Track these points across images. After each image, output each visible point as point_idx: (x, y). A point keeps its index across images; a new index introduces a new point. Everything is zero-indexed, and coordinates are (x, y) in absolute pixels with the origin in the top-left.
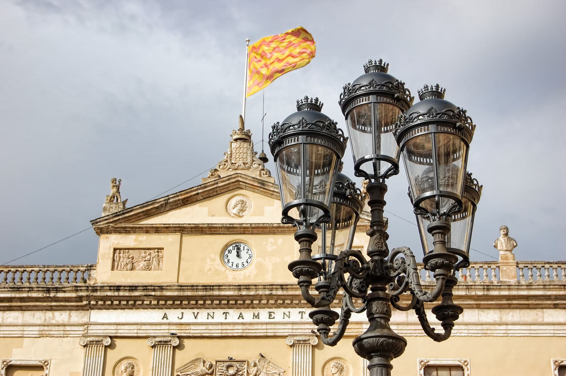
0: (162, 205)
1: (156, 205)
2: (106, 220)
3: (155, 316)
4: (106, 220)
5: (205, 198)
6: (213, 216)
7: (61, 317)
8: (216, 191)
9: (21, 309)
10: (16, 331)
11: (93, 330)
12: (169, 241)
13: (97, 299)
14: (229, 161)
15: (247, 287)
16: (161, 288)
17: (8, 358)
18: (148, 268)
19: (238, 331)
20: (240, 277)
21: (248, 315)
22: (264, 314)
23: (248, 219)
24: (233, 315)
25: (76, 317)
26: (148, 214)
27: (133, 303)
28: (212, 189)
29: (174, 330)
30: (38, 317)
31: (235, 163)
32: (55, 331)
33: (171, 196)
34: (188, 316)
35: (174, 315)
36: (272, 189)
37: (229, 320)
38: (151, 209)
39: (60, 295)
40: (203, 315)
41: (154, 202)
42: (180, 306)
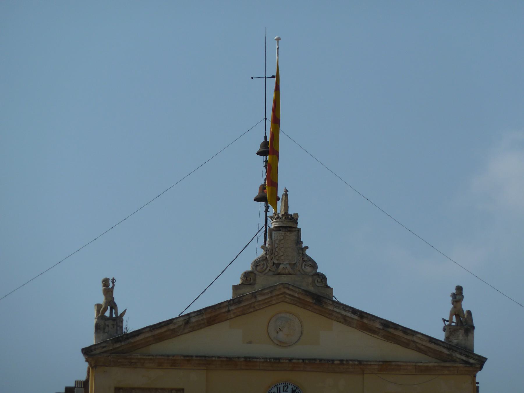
0: (180, 326)
1: (172, 327)
2: (104, 347)
4: (104, 347)
5: (238, 316)
6: (250, 342)
8: (254, 307)
14: (269, 259)
26: (160, 338)
28: (248, 304)
31: (280, 264)
33: (193, 315)
36: (331, 308)
38: (165, 332)
41: (171, 321)
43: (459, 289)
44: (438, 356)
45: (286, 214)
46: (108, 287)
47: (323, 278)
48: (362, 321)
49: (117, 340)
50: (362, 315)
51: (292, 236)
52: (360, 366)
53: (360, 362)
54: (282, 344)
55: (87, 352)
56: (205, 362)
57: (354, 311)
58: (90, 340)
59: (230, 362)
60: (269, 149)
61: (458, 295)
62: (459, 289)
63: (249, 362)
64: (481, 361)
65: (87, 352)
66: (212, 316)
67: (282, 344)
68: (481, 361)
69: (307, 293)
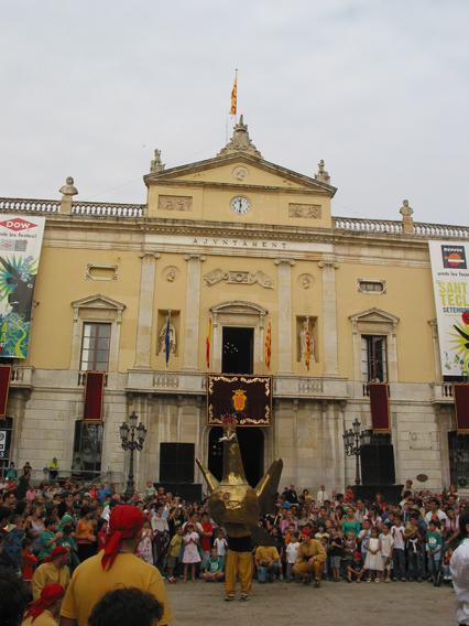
3: (188, 240)
7: (125, 237)
9: (97, 230)
10: (96, 245)
11: (147, 247)
12: (196, 193)
13: (151, 227)
15: (251, 225)
16: (194, 222)
17: (91, 263)
18: (181, 209)
19: (243, 253)
20: (243, 219)
21: (250, 244)
22: (260, 244)
23: (246, 182)
24: (240, 243)
25: (136, 238)
26: (181, 174)
27: (174, 231)
29: (202, 251)
30: (111, 237)
32: (123, 247)
34: (210, 242)
35: (201, 241)
37: (237, 246)
39: (125, 223)
40: (220, 242)
42: (205, 235)
43: (322, 161)
44: (314, 186)
45: (242, 124)
46: (157, 153)
47: (259, 153)
48: (278, 171)
49: (160, 173)
50: (278, 167)
51: (245, 135)
52: (276, 190)
53: (278, 188)
54: (239, 179)
55: (145, 177)
56: (204, 185)
57: (274, 166)
58: (148, 172)
59: (214, 186)
60: (234, 96)
61: (322, 165)
62: (322, 161)
63: (224, 187)
64: (335, 190)
65: (145, 177)
66: (206, 166)
67: (239, 179)
68: (335, 190)
69: (252, 157)
